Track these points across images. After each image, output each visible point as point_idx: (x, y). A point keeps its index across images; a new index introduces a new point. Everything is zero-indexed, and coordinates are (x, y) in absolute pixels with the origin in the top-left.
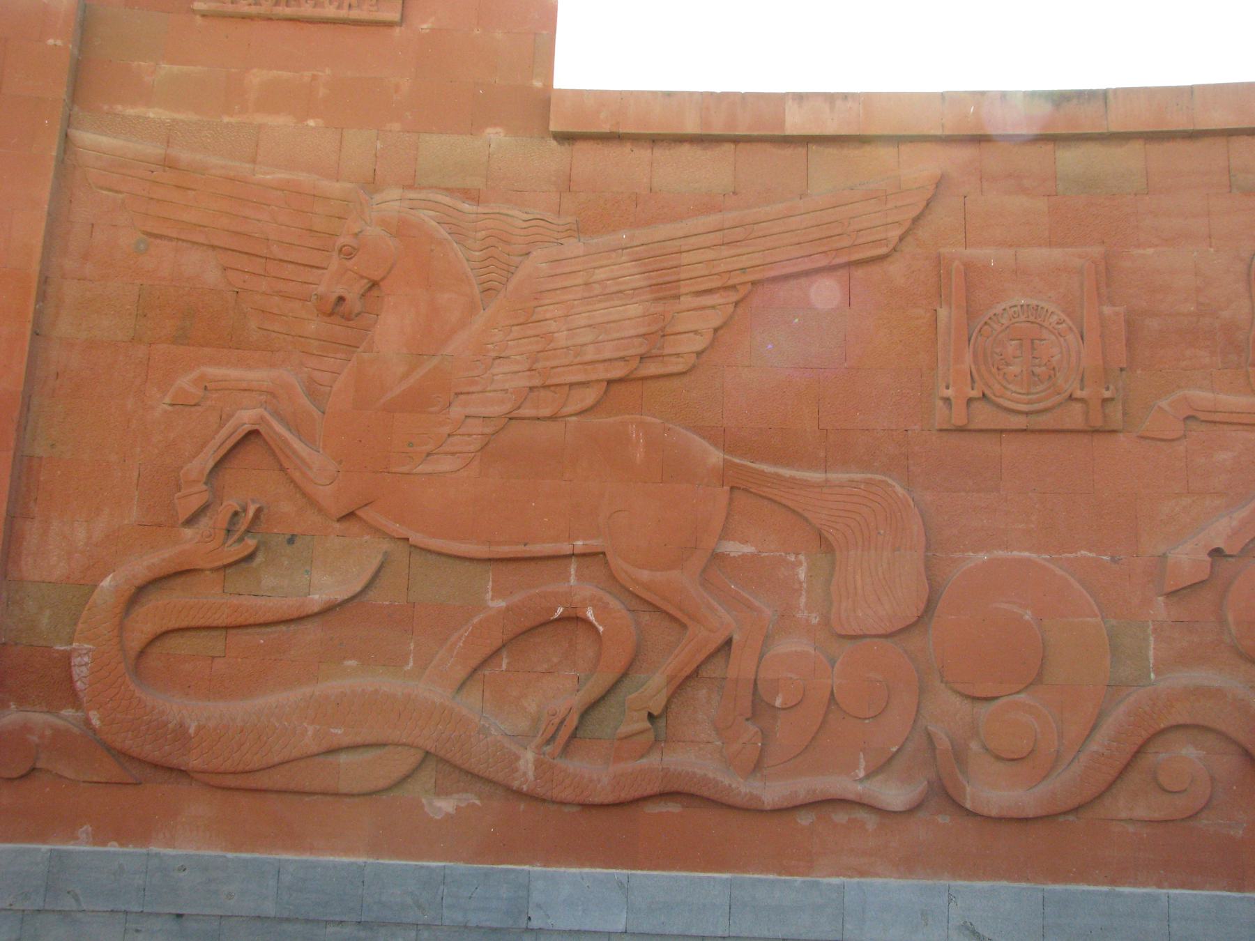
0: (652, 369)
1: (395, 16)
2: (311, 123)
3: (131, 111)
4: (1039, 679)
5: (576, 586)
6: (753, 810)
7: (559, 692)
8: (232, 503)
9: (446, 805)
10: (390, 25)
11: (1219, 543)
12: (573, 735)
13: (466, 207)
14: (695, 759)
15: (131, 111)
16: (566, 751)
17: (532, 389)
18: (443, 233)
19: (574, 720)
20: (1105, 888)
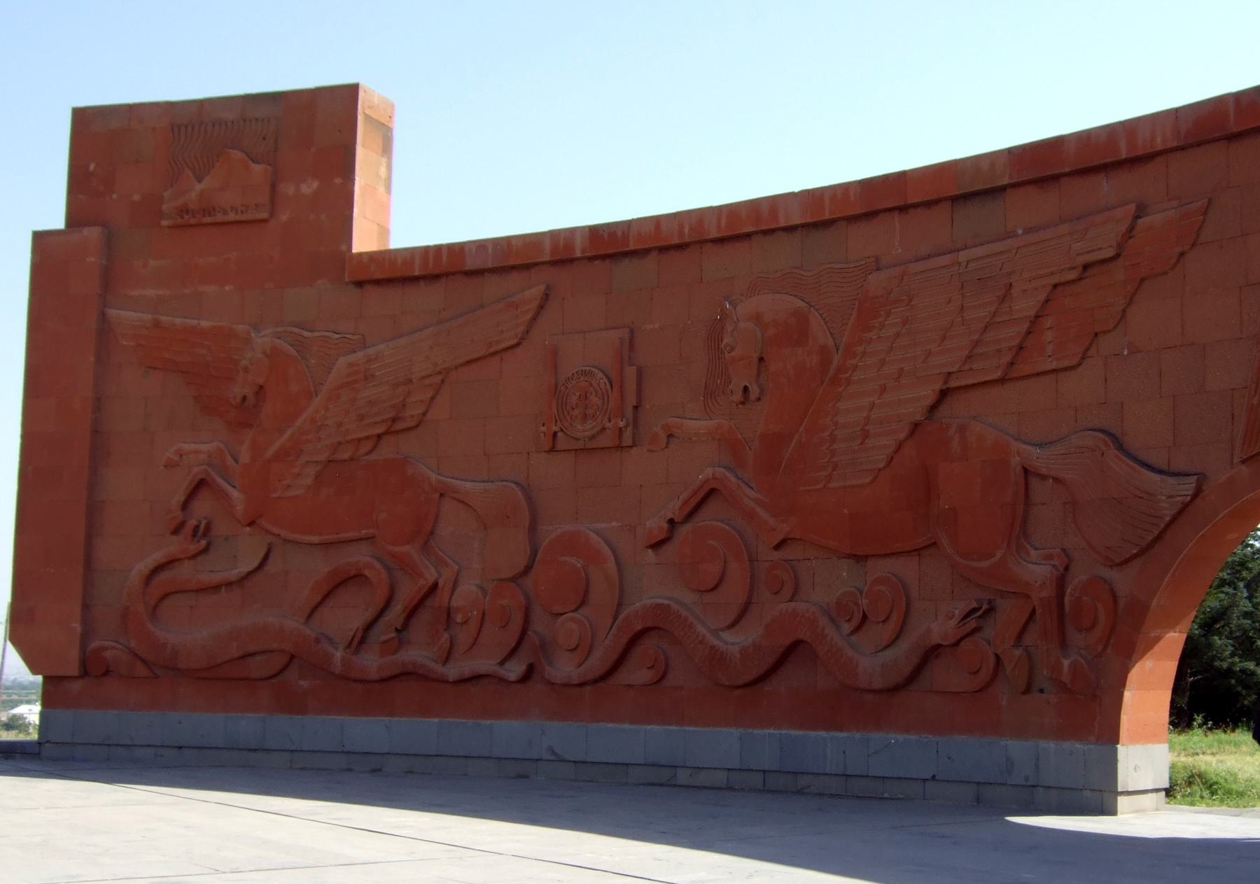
0: (399, 426)
1: (264, 215)
2: (227, 288)
3: (135, 293)
4: (583, 603)
5: (359, 556)
6: (443, 681)
7: (346, 617)
8: (192, 523)
9: (304, 684)
10: (264, 221)
11: (670, 516)
12: (360, 641)
13: (305, 334)
14: (417, 654)
15: (135, 293)
16: (357, 651)
17: (340, 443)
18: (292, 351)
19: (359, 635)
20: (617, 726)
